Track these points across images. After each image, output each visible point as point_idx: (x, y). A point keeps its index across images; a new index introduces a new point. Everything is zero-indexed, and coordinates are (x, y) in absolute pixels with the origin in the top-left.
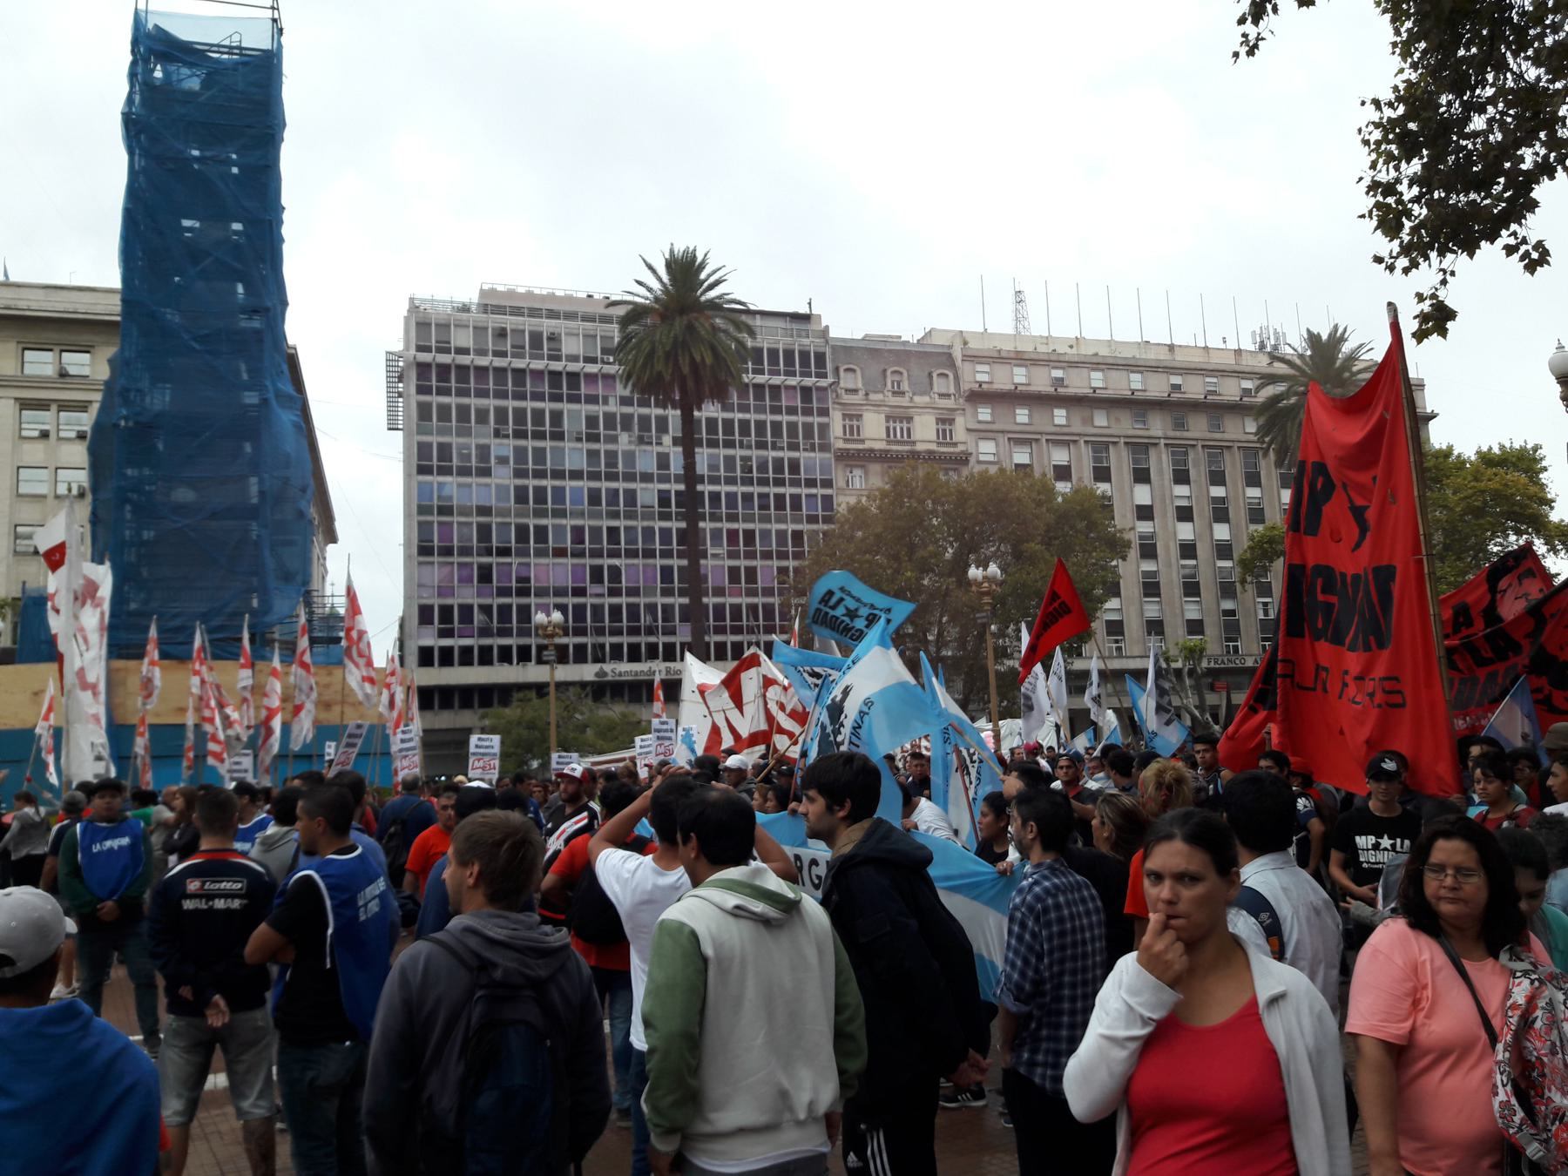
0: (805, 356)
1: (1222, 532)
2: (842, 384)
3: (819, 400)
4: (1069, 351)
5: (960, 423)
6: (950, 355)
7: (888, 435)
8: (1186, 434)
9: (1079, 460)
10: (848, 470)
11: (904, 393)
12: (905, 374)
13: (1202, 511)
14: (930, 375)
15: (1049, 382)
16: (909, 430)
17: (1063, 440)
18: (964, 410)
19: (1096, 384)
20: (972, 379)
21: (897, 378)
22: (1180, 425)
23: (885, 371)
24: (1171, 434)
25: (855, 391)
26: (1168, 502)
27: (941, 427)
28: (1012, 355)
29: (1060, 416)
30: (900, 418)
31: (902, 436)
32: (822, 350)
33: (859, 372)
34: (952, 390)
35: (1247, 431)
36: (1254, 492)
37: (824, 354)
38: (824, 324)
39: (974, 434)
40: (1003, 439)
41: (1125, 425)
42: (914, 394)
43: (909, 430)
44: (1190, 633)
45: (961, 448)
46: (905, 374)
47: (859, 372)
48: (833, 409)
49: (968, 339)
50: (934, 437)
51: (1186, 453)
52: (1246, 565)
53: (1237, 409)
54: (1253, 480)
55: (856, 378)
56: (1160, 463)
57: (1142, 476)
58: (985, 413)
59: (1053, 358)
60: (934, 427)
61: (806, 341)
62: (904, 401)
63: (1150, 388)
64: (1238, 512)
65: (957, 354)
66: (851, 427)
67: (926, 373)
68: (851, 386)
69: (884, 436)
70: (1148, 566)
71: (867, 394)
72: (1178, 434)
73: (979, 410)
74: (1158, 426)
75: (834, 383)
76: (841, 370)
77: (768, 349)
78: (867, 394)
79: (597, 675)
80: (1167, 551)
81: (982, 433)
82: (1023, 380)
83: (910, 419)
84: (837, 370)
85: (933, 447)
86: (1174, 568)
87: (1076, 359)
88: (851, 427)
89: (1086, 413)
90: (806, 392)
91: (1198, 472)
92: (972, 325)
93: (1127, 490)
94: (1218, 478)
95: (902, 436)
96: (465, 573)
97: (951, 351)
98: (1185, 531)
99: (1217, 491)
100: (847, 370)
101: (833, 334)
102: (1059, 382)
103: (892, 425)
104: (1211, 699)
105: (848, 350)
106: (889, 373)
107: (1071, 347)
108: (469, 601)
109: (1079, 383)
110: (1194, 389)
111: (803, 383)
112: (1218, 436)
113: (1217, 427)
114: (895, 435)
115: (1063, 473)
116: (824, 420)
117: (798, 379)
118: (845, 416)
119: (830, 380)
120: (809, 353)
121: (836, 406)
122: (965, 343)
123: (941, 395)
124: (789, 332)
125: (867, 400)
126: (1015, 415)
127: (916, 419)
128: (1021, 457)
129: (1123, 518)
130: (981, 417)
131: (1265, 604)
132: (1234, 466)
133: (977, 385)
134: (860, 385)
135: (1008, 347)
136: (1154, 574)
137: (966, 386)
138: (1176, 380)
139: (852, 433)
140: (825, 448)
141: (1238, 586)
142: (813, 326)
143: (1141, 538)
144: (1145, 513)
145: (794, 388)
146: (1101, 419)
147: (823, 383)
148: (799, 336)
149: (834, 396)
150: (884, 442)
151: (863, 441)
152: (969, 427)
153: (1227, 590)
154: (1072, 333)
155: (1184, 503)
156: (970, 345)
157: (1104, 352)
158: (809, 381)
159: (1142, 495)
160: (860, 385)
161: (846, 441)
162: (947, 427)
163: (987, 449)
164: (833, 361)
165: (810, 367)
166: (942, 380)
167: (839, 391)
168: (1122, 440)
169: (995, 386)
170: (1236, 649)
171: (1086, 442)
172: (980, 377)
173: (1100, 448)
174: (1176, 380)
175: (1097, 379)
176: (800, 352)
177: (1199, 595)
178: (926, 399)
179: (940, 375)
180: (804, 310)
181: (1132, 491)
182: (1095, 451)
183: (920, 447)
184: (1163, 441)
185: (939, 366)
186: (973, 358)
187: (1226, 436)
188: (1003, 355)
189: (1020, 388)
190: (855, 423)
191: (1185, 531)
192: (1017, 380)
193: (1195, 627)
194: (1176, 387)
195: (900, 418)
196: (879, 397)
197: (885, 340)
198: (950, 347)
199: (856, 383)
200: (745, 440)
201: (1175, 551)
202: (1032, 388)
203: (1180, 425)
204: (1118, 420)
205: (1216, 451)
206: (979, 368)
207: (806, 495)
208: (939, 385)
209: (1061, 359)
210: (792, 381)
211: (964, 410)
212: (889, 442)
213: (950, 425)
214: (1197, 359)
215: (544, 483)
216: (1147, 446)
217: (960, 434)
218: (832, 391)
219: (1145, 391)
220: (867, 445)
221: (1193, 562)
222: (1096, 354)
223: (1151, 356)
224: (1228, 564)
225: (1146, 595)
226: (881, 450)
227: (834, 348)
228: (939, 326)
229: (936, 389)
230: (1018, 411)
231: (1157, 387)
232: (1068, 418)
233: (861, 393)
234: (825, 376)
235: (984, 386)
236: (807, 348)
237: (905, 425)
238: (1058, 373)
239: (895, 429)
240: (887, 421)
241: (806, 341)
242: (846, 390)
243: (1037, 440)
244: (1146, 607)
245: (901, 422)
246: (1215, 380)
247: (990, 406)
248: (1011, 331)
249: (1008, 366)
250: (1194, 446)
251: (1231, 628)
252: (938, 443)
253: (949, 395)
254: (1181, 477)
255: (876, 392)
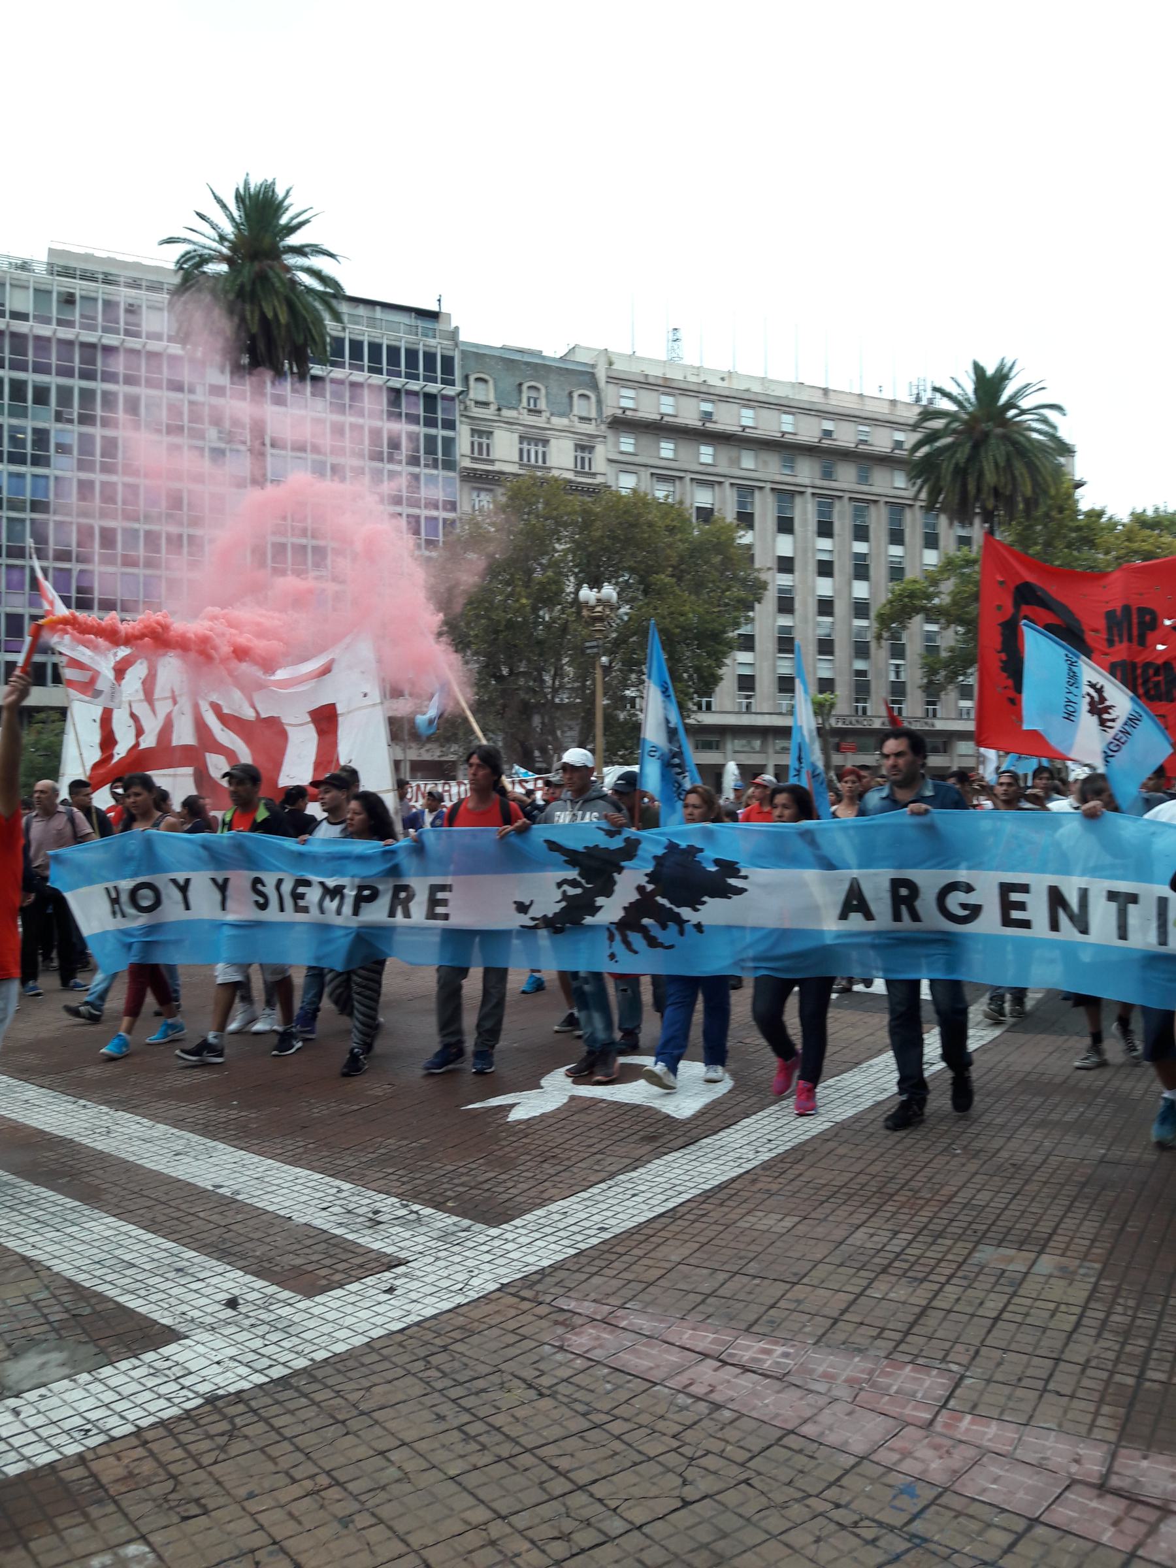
0: (430, 357)
1: (861, 590)
2: (472, 395)
3: (444, 410)
4: (719, 383)
5: (601, 453)
6: (593, 375)
7: (521, 458)
8: (834, 484)
9: (723, 501)
10: (475, 494)
11: (540, 412)
12: (543, 391)
13: (844, 567)
14: (570, 395)
15: (696, 416)
16: (544, 453)
17: (706, 481)
18: (605, 437)
19: (745, 422)
20: (615, 405)
21: (533, 394)
22: (828, 474)
23: (520, 385)
24: (819, 483)
25: (485, 404)
26: (810, 555)
27: (579, 454)
28: (660, 382)
29: (706, 453)
30: (535, 439)
31: (537, 461)
32: (450, 353)
33: (491, 383)
34: (593, 415)
35: (897, 485)
36: (896, 551)
37: (452, 359)
38: (453, 325)
39: (614, 465)
40: (645, 474)
41: (771, 469)
42: (552, 415)
43: (544, 453)
44: (821, 692)
45: (599, 480)
46: (543, 391)
47: (491, 383)
48: (461, 422)
49: (614, 359)
50: (572, 466)
51: (831, 505)
52: (884, 620)
53: (885, 461)
54: (897, 537)
55: (487, 390)
56: (805, 513)
57: (785, 526)
58: (627, 444)
59: (704, 389)
60: (573, 454)
61: (432, 342)
62: (540, 421)
63: (800, 432)
64: (879, 571)
65: (601, 374)
66: (480, 445)
67: (567, 392)
68: (482, 398)
69: (516, 459)
70: (785, 621)
71: (499, 410)
72: (825, 483)
73: (622, 440)
74: (806, 473)
75: (462, 392)
76: (472, 378)
77: (388, 347)
78: (499, 410)
80: (805, 605)
81: (623, 464)
82: (670, 411)
83: (546, 442)
84: (466, 378)
85: (570, 476)
86: (811, 624)
87: (727, 394)
88: (480, 445)
89: (733, 452)
90: (430, 399)
91: (842, 522)
92: (619, 346)
93: (769, 538)
94: (861, 533)
95: (537, 461)
96: (15, 576)
97: (595, 371)
98: (825, 587)
99: (860, 547)
100: (478, 379)
101: (463, 337)
102: (707, 416)
103: (525, 446)
104: (837, 759)
105: (479, 357)
106: (525, 387)
107: (723, 379)
108: (19, 611)
109: (728, 419)
110: (846, 436)
111: (427, 389)
112: (865, 488)
113: (864, 478)
114: (529, 460)
115: (705, 514)
116: (449, 433)
117: (422, 383)
118: (474, 432)
119: (458, 388)
120: (434, 355)
121: (463, 419)
122: (611, 364)
123: (582, 419)
124: (414, 330)
126: (659, 448)
127: (553, 442)
128: (661, 492)
129: (763, 560)
130: (624, 448)
131: (898, 666)
132: (878, 521)
133: (620, 411)
134: (491, 397)
135: (655, 372)
136: (788, 629)
137: (609, 411)
138: (828, 425)
139: (480, 452)
140: (449, 465)
141: (873, 645)
142: (441, 326)
143: (780, 591)
144: (786, 565)
145: (416, 394)
146: (748, 461)
147: (450, 391)
148: (427, 336)
149: (462, 407)
150: (517, 466)
151: (492, 462)
152: (611, 457)
153: (861, 650)
154: (724, 366)
155: (825, 557)
156: (614, 367)
157: (757, 388)
158: (433, 388)
159: (785, 546)
160: (491, 397)
161: (474, 459)
162: (586, 455)
163: (626, 483)
164: (463, 367)
165: (435, 372)
166: (584, 402)
167: (468, 403)
168: (769, 486)
169: (640, 415)
170: (864, 710)
171: (732, 484)
172: (625, 403)
173: (746, 491)
174: (828, 425)
175: (747, 417)
176: (425, 353)
177: (831, 653)
178: (564, 421)
179: (581, 396)
180: (434, 307)
181: (774, 541)
182: (740, 496)
183: (555, 473)
184: (810, 490)
185: (581, 385)
186: (618, 380)
187: (874, 490)
188: (651, 380)
189: (666, 419)
190: (484, 441)
191: (825, 587)
192: (665, 410)
193: (826, 685)
194: (828, 433)
195: (535, 439)
196: (513, 413)
197: (521, 351)
198: (593, 366)
199: (487, 395)
201: (813, 607)
202: (679, 420)
203: (828, 474)
204: (765, 463)
205: (862, 504)
206: (625, 392)
207: (426, 518)
208: (580, 408)
209: (712, 391)
210: (414, 386)
211: (605, 437)
212: (521, 465)
214: (851, 405)
215: (113, 478)
216: (792, 494)
217: (599, 462)
218: (461, 402)
219: (795, 434)
220: (497, 467)
221: (829, 619)
222: (747, 390)
223: (805, 397)
224: (863, 623)
225: (781, 651)
227: (463, 352)
228: (582, 344)
229: (576, 411)
230: (663, 445)
231: (808, 431)
232: (714, 456)
233: (493, 407)
234: (452, 383)
235: (628, 413)
236: (433, 350)
237: (540, 449)
238: (707, 407)
239: (529, 451)
240: (521, 443)
241: (432, 342)
242: (477, 403)
243: (681, 478)
244: (780, 663)
246: (866, 429)
247: (633, 436)
248: (663, 357)
249: (655, 394)
250: (840, 497)
251: (862, 689)
252: (576, 472)
253: (590, 420)
254: (825, 530)
255: (510, 408)
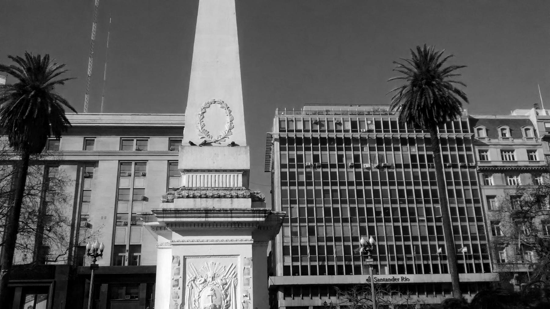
7: (503, 159)
31: (510, 159)
43: (513, 156)
62: (509, 142)
69: (501, 159)
79: (367, 280)
85: (527, 164)
95: (510, 159)
125: (490, 142)
152: (545, 153)
183: (520, 164)
200: (431, 164)
213: (534, 152)
220: (493, 164)
226: (501, 166)
245: (509, 152)
253: (532, 138)
